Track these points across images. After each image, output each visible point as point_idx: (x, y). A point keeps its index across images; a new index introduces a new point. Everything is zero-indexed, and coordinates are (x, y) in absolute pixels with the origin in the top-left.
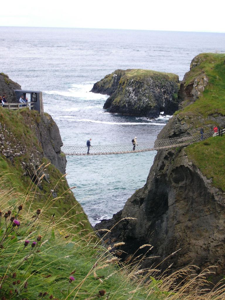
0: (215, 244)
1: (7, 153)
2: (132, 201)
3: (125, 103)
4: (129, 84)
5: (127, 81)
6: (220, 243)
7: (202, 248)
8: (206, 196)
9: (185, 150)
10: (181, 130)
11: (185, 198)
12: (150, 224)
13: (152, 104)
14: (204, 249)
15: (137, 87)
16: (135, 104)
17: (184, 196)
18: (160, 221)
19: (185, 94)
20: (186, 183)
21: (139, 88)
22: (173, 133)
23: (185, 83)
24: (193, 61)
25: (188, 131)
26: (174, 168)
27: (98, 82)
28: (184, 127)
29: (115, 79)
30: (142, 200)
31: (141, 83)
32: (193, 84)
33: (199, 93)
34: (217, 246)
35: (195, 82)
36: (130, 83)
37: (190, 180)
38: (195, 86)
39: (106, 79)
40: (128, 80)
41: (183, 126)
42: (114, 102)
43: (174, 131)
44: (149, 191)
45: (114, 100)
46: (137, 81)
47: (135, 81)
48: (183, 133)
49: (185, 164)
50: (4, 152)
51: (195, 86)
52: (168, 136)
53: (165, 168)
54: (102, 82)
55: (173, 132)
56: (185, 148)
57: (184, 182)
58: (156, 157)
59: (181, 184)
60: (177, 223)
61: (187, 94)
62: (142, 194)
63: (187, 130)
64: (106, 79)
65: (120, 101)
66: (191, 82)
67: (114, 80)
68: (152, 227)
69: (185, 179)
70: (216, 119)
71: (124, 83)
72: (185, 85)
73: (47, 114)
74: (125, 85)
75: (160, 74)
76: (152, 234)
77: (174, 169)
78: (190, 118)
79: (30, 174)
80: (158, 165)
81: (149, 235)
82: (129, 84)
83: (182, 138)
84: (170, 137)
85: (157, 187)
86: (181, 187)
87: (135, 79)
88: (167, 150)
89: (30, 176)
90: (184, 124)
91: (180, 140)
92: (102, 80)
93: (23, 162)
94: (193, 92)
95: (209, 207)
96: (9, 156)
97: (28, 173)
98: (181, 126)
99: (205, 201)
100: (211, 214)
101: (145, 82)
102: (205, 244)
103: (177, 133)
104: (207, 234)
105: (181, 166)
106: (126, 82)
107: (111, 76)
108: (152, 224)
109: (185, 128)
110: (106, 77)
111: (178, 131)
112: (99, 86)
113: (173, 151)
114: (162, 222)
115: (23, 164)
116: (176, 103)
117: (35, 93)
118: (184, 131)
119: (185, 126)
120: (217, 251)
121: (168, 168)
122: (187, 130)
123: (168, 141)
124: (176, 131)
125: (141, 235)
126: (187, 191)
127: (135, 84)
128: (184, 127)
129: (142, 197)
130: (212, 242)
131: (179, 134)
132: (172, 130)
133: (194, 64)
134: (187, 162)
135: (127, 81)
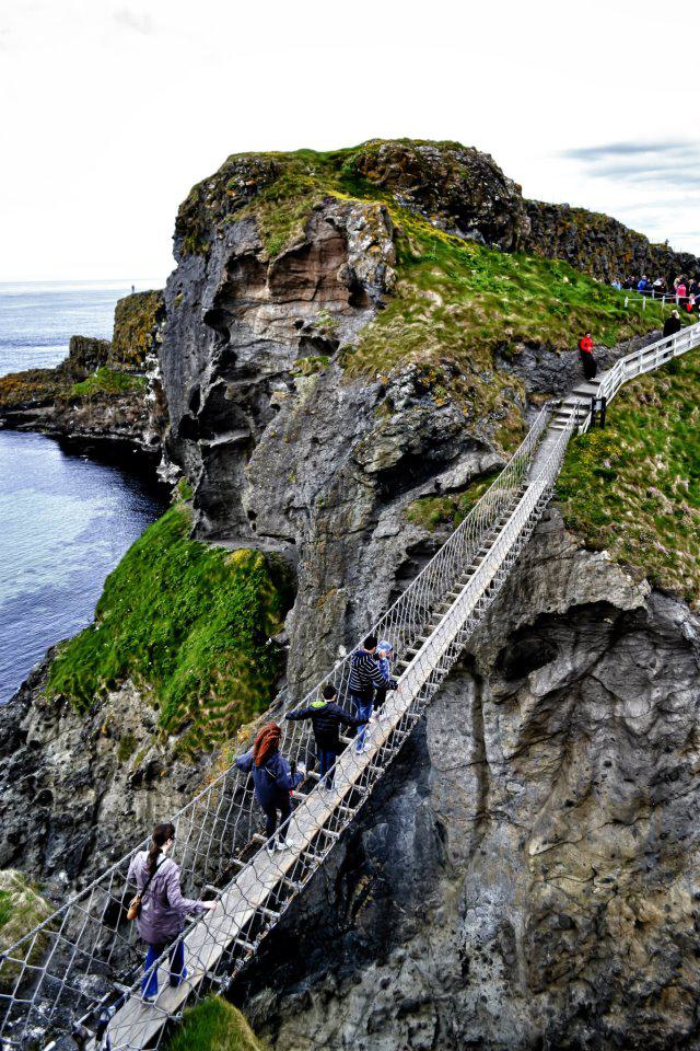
10: (435, 431)
22: (399, 454)
23: (258, 250)
25: (466, 432)
28: (451, 418)
38: (367, 243)
41: (447, 411)
43: (403, 442)
48: (444, 441)
49: (616, 598)
55: (401, 446)
63: (458, 431)
76: (365, 893)
90: (447, 406)
98: (437, 414)
103: (415, 452)
109: (456, 419)
111: (423, 438)
122: (458, 431)
124: (415, 442)
128: (451, 418)
132: (394, 439)
133: (242, 183)
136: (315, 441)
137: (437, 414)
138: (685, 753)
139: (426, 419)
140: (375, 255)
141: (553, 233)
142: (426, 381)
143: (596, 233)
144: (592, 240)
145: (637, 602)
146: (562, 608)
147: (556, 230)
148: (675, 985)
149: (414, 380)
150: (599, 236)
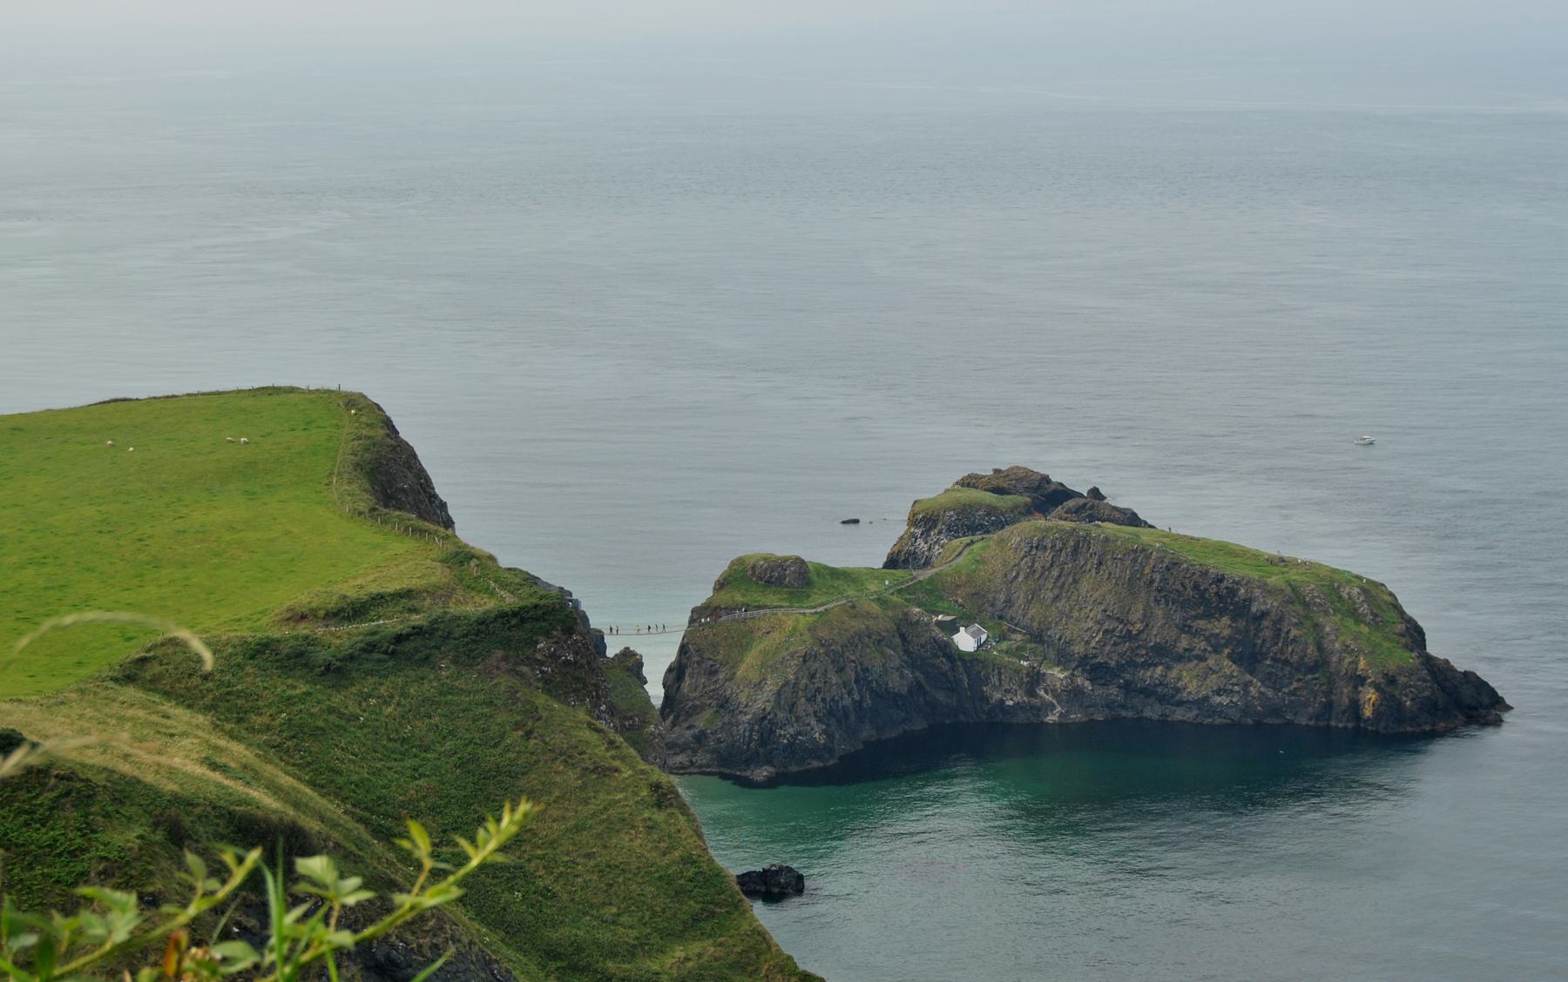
12: (677, 685)
15: (927, 527)
21: (931, 529)
31: (934, 521)
47: (924, 517)
75: (965, 505)
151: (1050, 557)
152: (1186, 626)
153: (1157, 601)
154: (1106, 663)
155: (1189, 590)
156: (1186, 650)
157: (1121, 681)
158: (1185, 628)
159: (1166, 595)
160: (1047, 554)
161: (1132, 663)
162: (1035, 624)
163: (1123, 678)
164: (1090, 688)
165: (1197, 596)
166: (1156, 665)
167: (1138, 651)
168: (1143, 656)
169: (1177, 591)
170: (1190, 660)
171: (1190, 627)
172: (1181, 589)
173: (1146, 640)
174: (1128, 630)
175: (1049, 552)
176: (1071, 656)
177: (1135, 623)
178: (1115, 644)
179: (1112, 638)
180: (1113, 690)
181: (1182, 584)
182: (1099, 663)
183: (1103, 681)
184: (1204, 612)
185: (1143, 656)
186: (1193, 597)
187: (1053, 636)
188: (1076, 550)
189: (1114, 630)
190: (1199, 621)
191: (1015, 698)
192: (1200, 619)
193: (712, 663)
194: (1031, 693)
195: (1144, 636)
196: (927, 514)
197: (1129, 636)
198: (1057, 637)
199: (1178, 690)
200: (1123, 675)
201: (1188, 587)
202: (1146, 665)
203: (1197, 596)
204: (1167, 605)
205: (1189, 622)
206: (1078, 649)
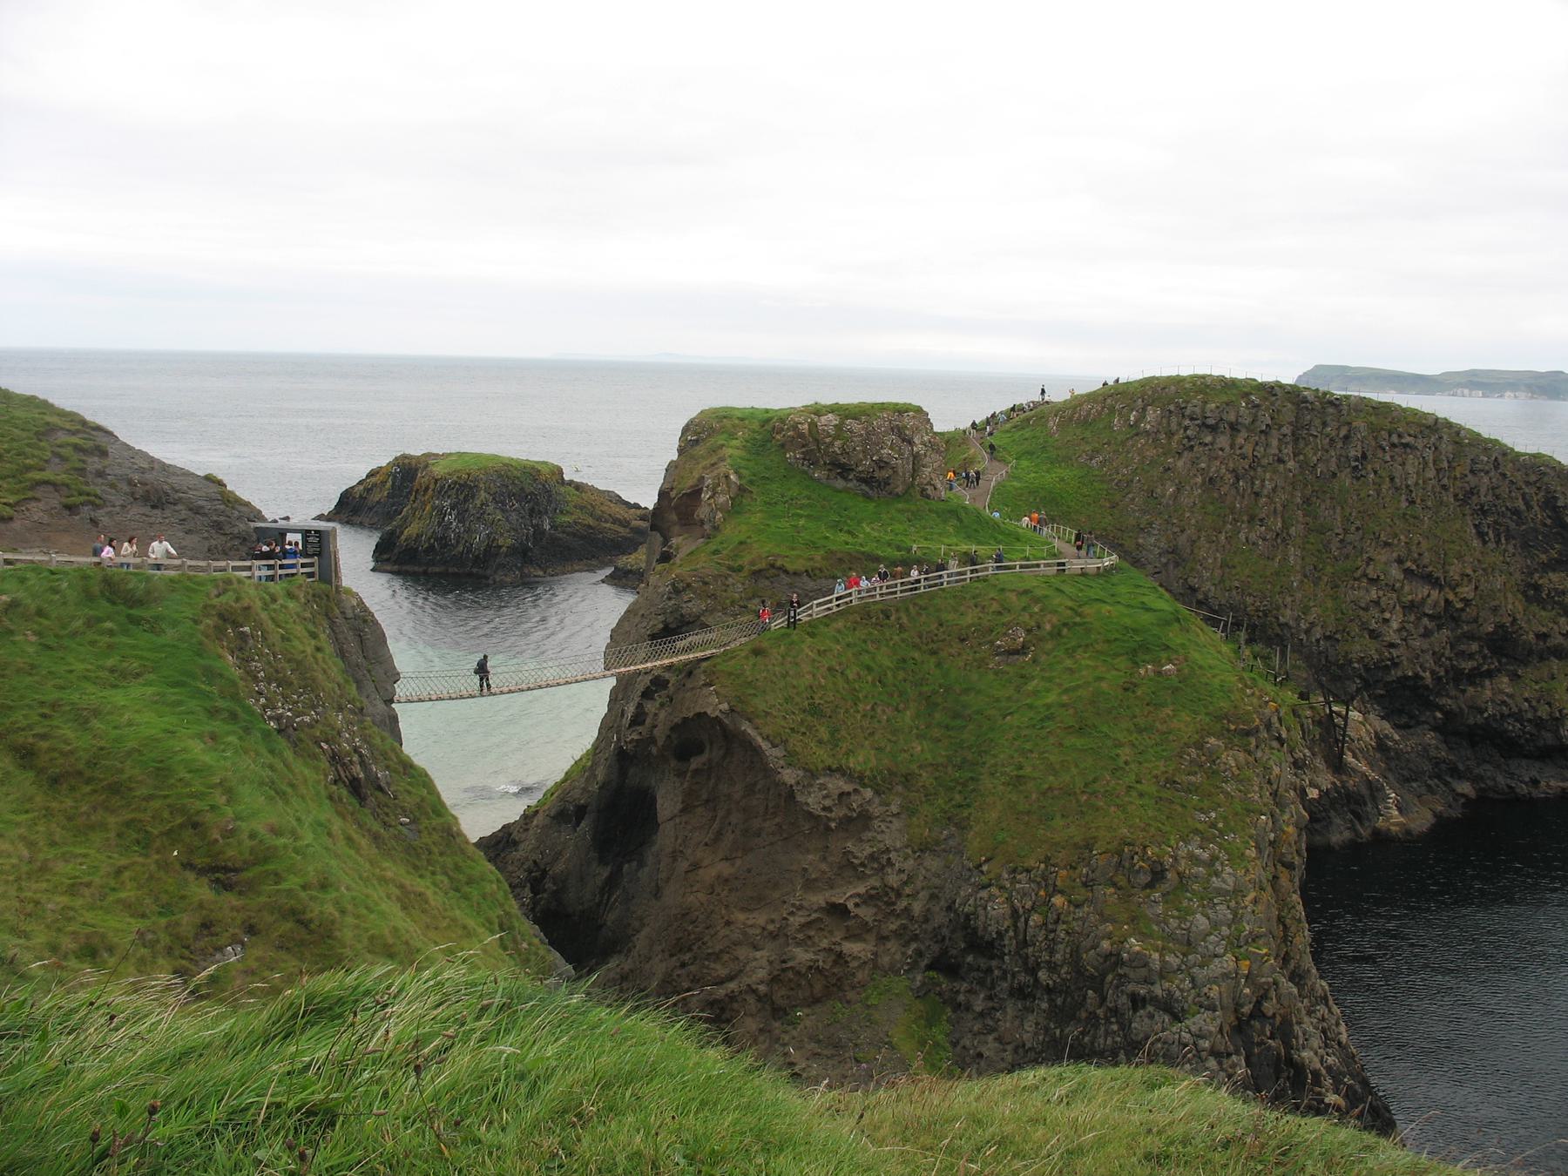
0: (803, 920)
1: (278, 719)
2: (552, 814)
3: (432, 541)
4: (439, 492)
5: (436, 483)
6: (814, 916)
7: (765, 933)
8: (771, 792)
9: (705, 672)
10: (682, 615)
11: (707, 801)
12: (605, 872)
13: (501, 542)
14: (771, 933)
15: (461, 497)
16: (458, 542)
17: (705, 797)
18: (634, 864)
19: (674, 517)
20: (710, 760)
21: (466, 500)
22: (661, 626)
23: (672, 489)
24: (685, 430)
26: (676, 720)
27: (352, 488)
29: (395, 477)
30: (581, 812)
31: (471, 488)
32: (699, 491)
33: (720, 515)
34: (809, 925)
35: (707, 487)
36: (442, 487)
37: (721, 752)
39: (373, 480)
40: (436, 480)
41: (690, 605)
42: (403, 537)
44: (600, 784)
45: (402, 533)
46: (462, 482)
48: (689, 623)
50: (271, 718)
51: (705, 496)
52: (648, 633)
53: (647, 722)
54: (361, 488)
56: (704, 664)
57: (703, 758)
58: (614, 692)
59: (695, 763)
60: (691, 868)
61: (680, 519)
62: (582, 794)
63: (699, 617)
64: (373, 480)
65: (419, 536)
66: (692, 487)
67: (393, 483)
68: (612, 883)
69: (707, 751)
70: (772, 582)
71: (427, 489)
72: (673, 494)
73: (348, 591)
74: (430, 492)
76: (616, 900)
77: (677, 724)
78: (706, 583)
79: (343, 775)
80: (623, 715)
81: (606, 904)
82: (439, 492)
83: (690, 639)
84: (653, 637)
85: (623, 772)
86: (696, 772)
87: (455, 478)
88: (646, 673)
89: (344, 782)
91: (680, 644)
92: (360, 483)
93: (322, 744)
94: (702, 512)
95: (777, 820)
96: (283, 727)
97: (339, 775)
98: (684, 606)
99: (767, 805)
100: (786, 839)
101: (482, 485)
102: (773, 921)
103: (671, 626)
104: (776, 895)
105: (699, 715)
106: (432, 486)
107: (384, 471)
108: (611, 873)
110: (371, 474)
112: (354, 498)
113: (667, 675)
114: (641, 864)
115: (322, 748)
116: (561, 535)
117: (316, 532)
118: (691, 620)
119: (694, 606)
120: (810, 937)
121: (661, 717)
123: (644, 649)
124: (670, 620)
125: (582, 904)
126: (713, 781)
127: (458, 490)
129: (582, 802)
130: (792, 913)
131: (678, 627)
134: (713, 704)
135: (436, 483)
136: (643, 615)
137: (684, 606)
138: (765, 820)
139: (677, 608)
140: (710, 504)
141: (1334, 433)
142: (680, 586)
143: (1400, 436)
144: (1393, 445)
145: (717, 713)
146: (691, 715)
147: (1338, 429)
148: (728, 953)
149: (673, 585)
150: (1403, 441)
151: (1248, 449)
152: (1529, 585)
153: (1481, 535)
154: (1417, 676)
155: (1536, 508)
156: (1543, 637)
157: (1439, 715)
158: (1533, 593)
159: (1495, 522)
160: (1240, 441)
161: (1458, 677)
162: (1249, 600)
163: (1440, 708)
164: (1397, 737)
165: (1549, 522)
166: (1490, 674)
167: (1463, 647)
168: (1471, 656)
169: (1516, 512)
170: (1542, 659)
171: (1537, 588)
172: (1523, 507)
173: (1476, 620)
174: (1447, 601)
175: (1244, 434)
176: (1341, 667)
177: (1457, 585)
178: (1427, 634)
179: (1419, 619)
180: (1431, 738)
181: (1524, 496)
182: (1406, 678)
183: (1404, 720)
184: (1559, 553)
185: (1471, 656)
186: (1545, 525)
187: (1291, 623)
188: (1297, 427)
189: (1424, 600)
190: (1554, 576)
191: (1319, 780)
192: (1554, 570)
193: (843, 785)
194: (1338, 766)
195: (1471, 612)
196: (459, 478)
197: (1448, 615)
198: (1303, 626)
199: (1539, 723)
200: (1443, 701)
201: (1534, 503)
202: (1475, 677)
203: (1549, 522)
204: (1498, 542)
205: (1537, 576)
206: (1361, 648)
